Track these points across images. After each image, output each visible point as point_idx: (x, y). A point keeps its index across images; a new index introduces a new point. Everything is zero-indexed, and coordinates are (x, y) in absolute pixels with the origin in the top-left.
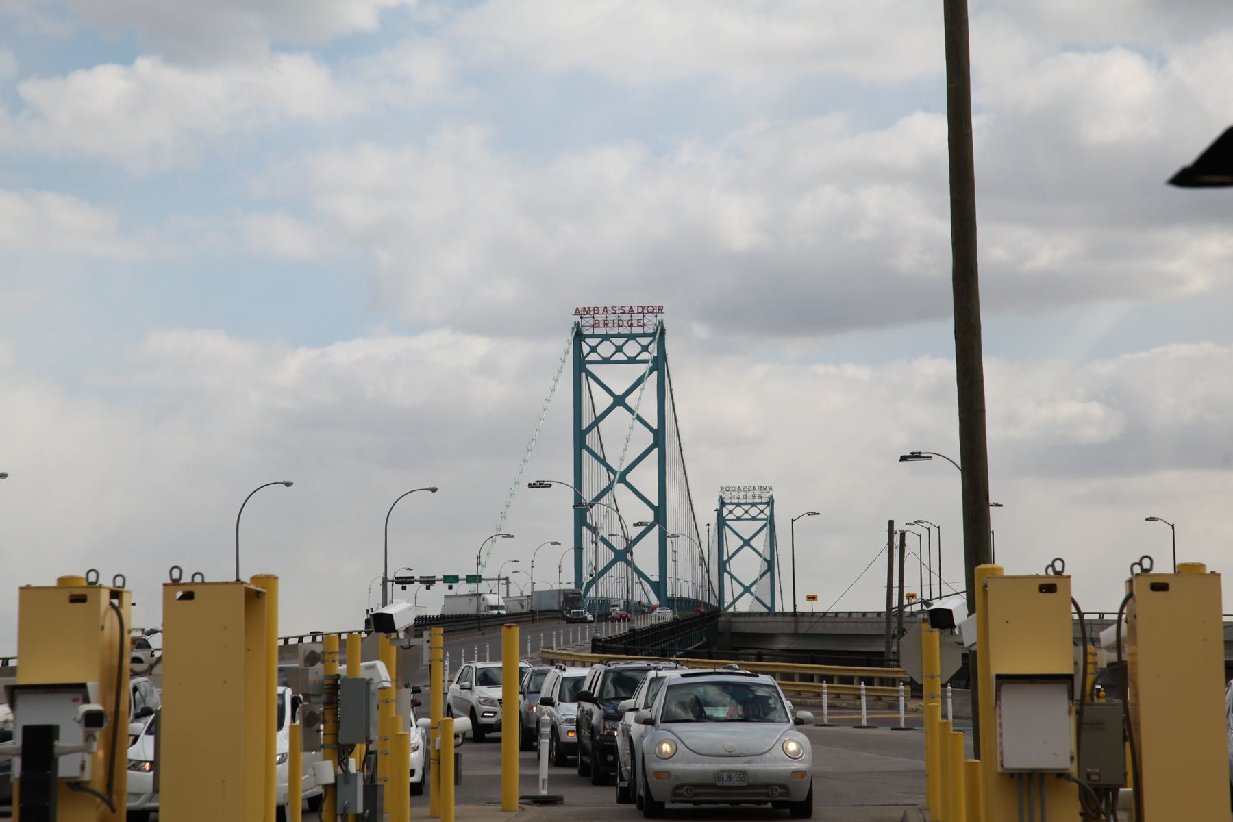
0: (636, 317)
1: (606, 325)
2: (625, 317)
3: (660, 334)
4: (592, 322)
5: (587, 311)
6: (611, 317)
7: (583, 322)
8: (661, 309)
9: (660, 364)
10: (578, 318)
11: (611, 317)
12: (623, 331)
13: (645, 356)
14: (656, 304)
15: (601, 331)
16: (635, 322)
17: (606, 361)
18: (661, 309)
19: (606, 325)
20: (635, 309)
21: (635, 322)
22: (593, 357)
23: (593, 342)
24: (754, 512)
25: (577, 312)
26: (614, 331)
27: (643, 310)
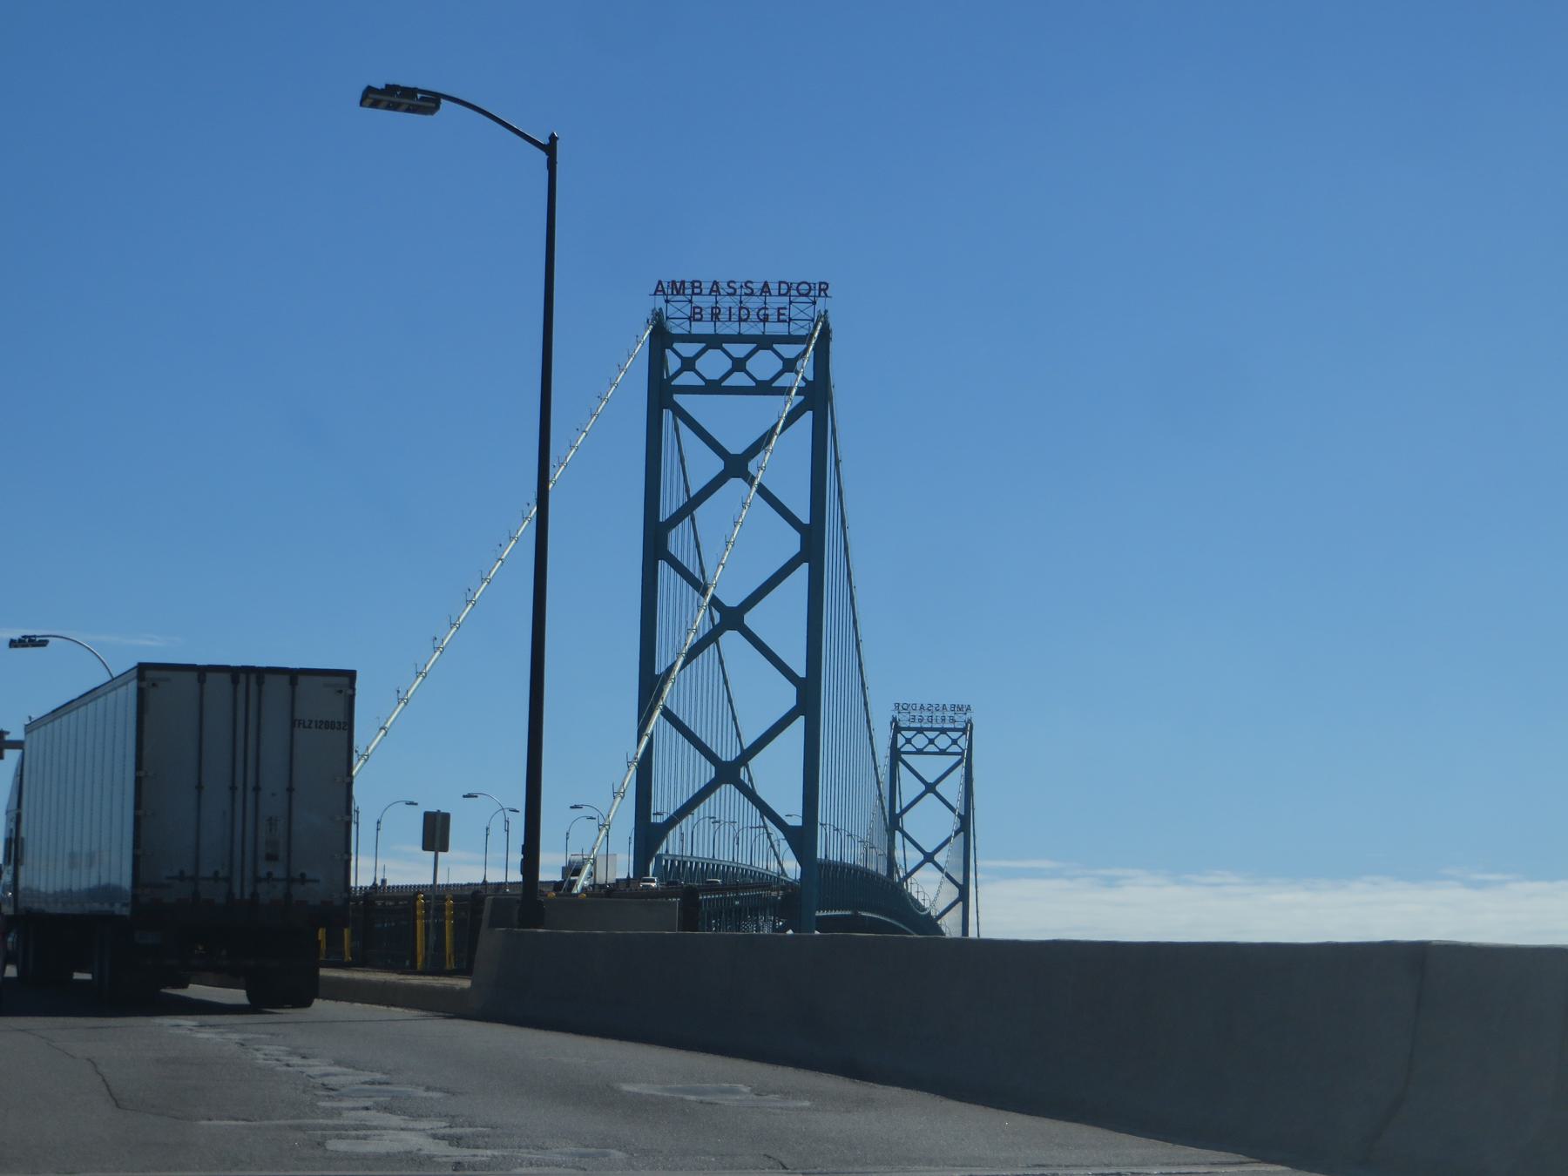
1: (715, 317)
6: (726, 302)
16: (773, 315)
17: (713, 387)
19: (715, 317)
20: (773, 287)
21: (773, 315)
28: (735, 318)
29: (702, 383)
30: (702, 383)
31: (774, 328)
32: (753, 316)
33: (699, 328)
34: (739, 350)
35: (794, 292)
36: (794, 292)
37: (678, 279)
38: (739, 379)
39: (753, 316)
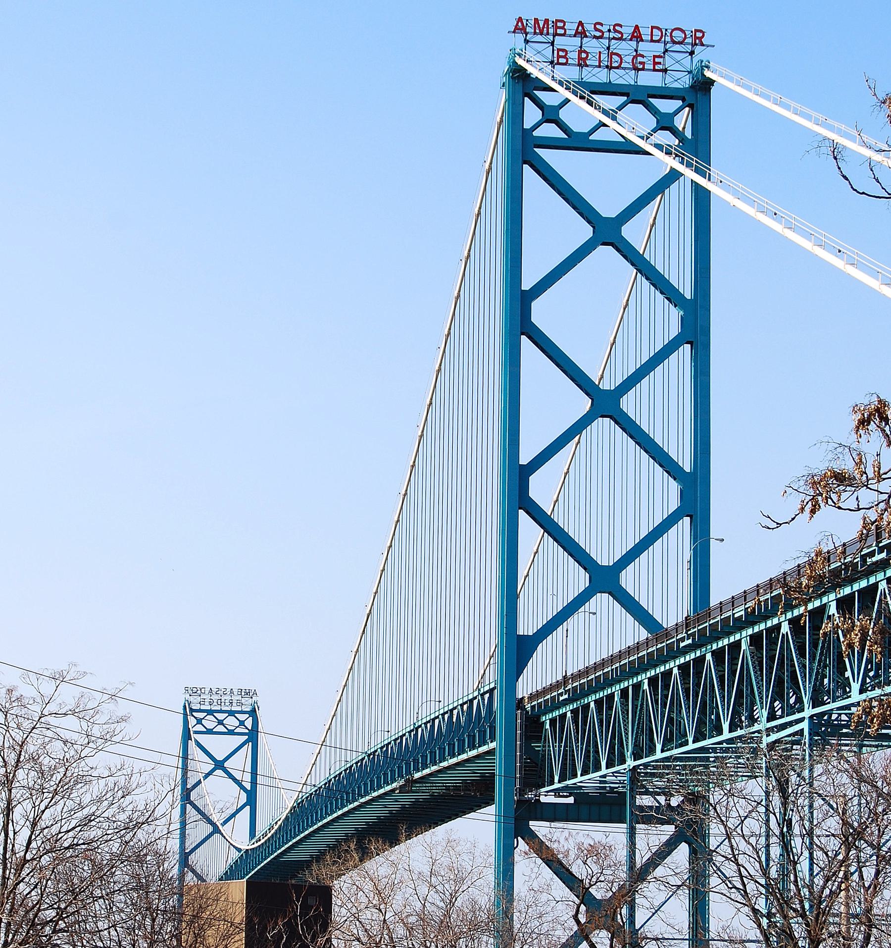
0: (649, 49)
5: (541, 27)
6: (592, 46)
8: (698, 39)
11: (592, 46)
12: (620, 78)
14: (689, 27)
18: (698, 39)
20: (645, 33)
22: (550, 131)
24: (232, 722)
25: (520, 27)
27: (661, 35)
31: (649, 79)
37: (541, 18)
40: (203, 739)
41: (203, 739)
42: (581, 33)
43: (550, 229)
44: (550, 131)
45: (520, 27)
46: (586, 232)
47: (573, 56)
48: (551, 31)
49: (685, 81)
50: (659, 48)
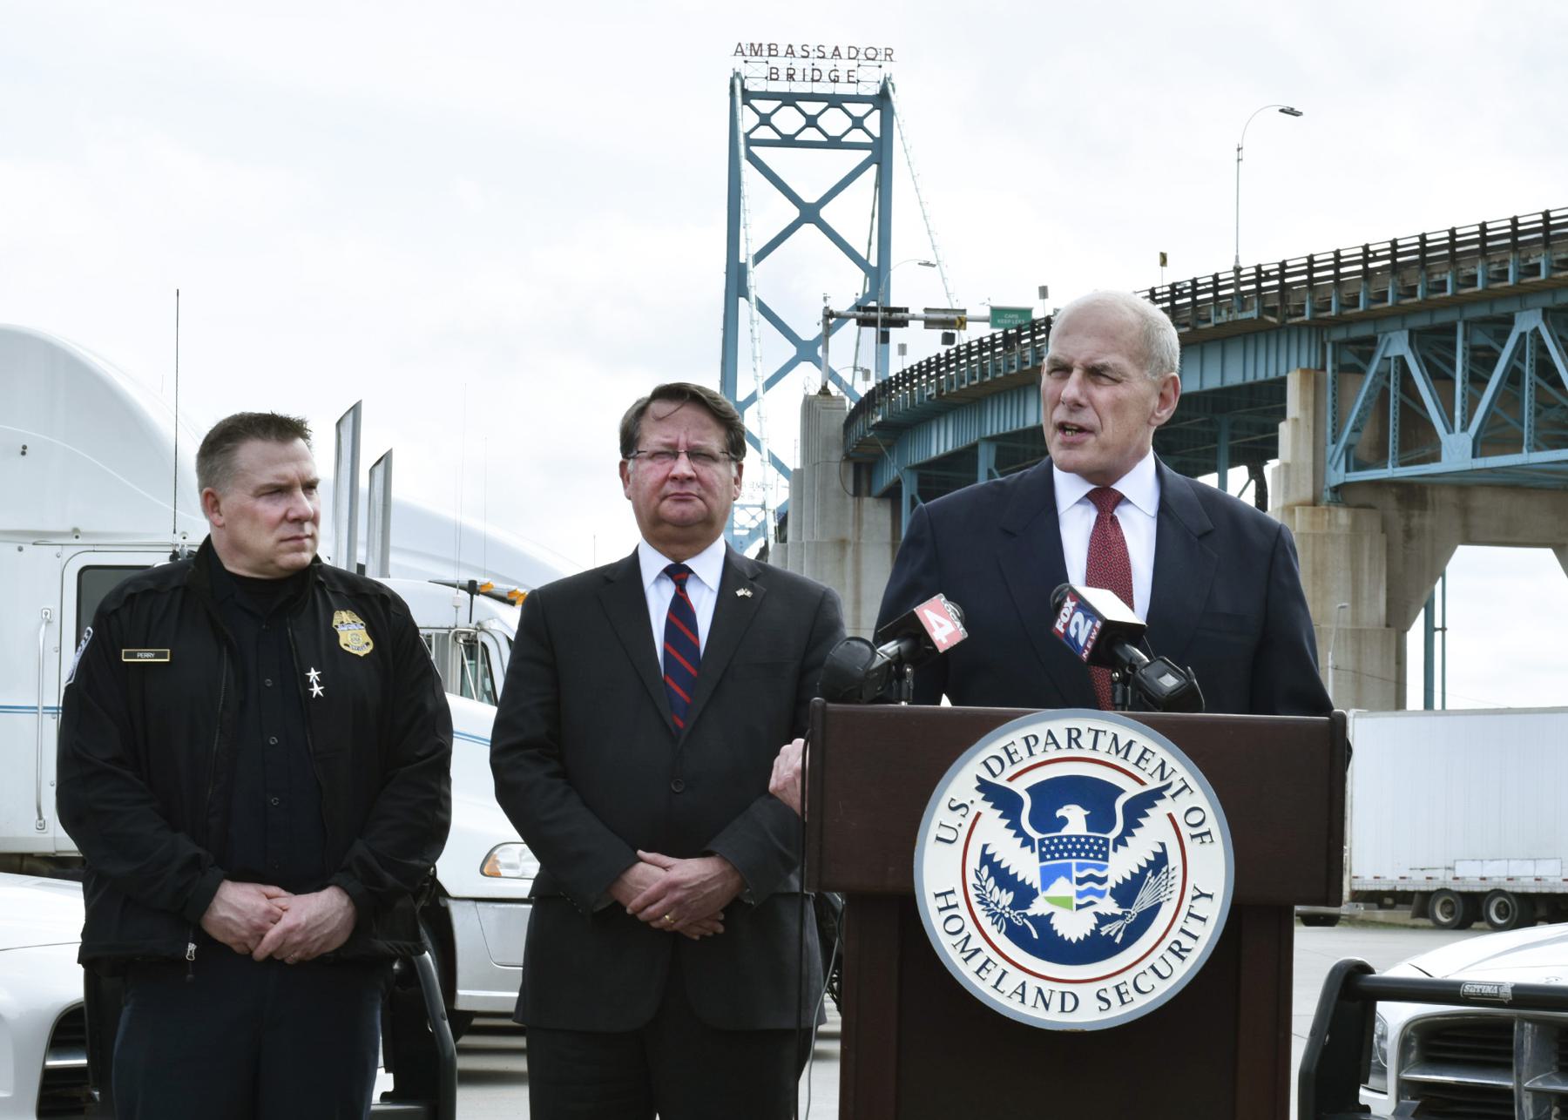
0: (844, 65)
1: (790, 77)
2: (825, 66)
3: (882, 100)
4: (766, 72)
5: (756, 50)
6: (799, 64)
7: (745, 71)
9: (880, 153)
10: (738, 63)
11: (799, 64)
12: (818, 89)
13: (857, 136)
14: (881, 46)
15: (782, 86)
16: (843, 78)
17: (788, 141)
18: (889, 55)
19: (790, 77)
21: (843, 78)
22: (765, 133)
23: (765, 106)
25: (739, 51)
26: (806, 88)
27: (855, 53)
28: (808, 78)
29: (778, 137)
30: (778, 137)
32: (825, 77)
33: (774, 87)
34: (812, 108)
35: (861, 56)
36: (861, 56)
38: (811, 134)
39: (825, 77)
40: (772, 157)
41: (772, 157)
42: (790, 52)
43: (766, 212)
44: (765, 133)
45: (739, 51)
46: (794, 213)
47: (783, 76)
48: (766, 53)
49: (874, 90)
50: (855, 62)
